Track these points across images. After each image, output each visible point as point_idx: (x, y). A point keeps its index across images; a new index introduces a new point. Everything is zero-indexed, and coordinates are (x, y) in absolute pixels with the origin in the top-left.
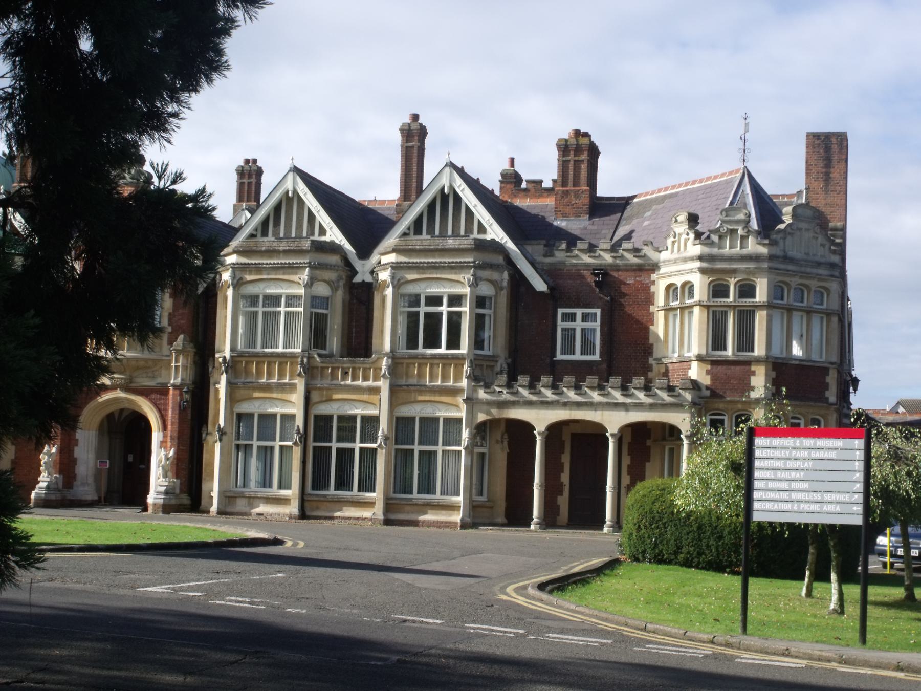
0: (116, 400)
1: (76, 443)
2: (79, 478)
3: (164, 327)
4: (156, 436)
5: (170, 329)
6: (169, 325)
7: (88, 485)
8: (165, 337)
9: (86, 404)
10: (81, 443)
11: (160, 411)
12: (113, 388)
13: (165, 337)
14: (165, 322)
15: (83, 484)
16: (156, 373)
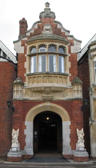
0: (45, 107)
1: (25, 127)
2: (27, 144)
3: (68, 74)
4: (66, 125)
5: (70, 75)
6: (70, 73)
7: (31, 147)
8: (68, 78)
9: (30, 109)
10: (27, 127)
11: (68, 111)
12: (44, 101)
13: (68, 78)
14: (68, 72)
15: (29, 147)
16: (65, 94)
